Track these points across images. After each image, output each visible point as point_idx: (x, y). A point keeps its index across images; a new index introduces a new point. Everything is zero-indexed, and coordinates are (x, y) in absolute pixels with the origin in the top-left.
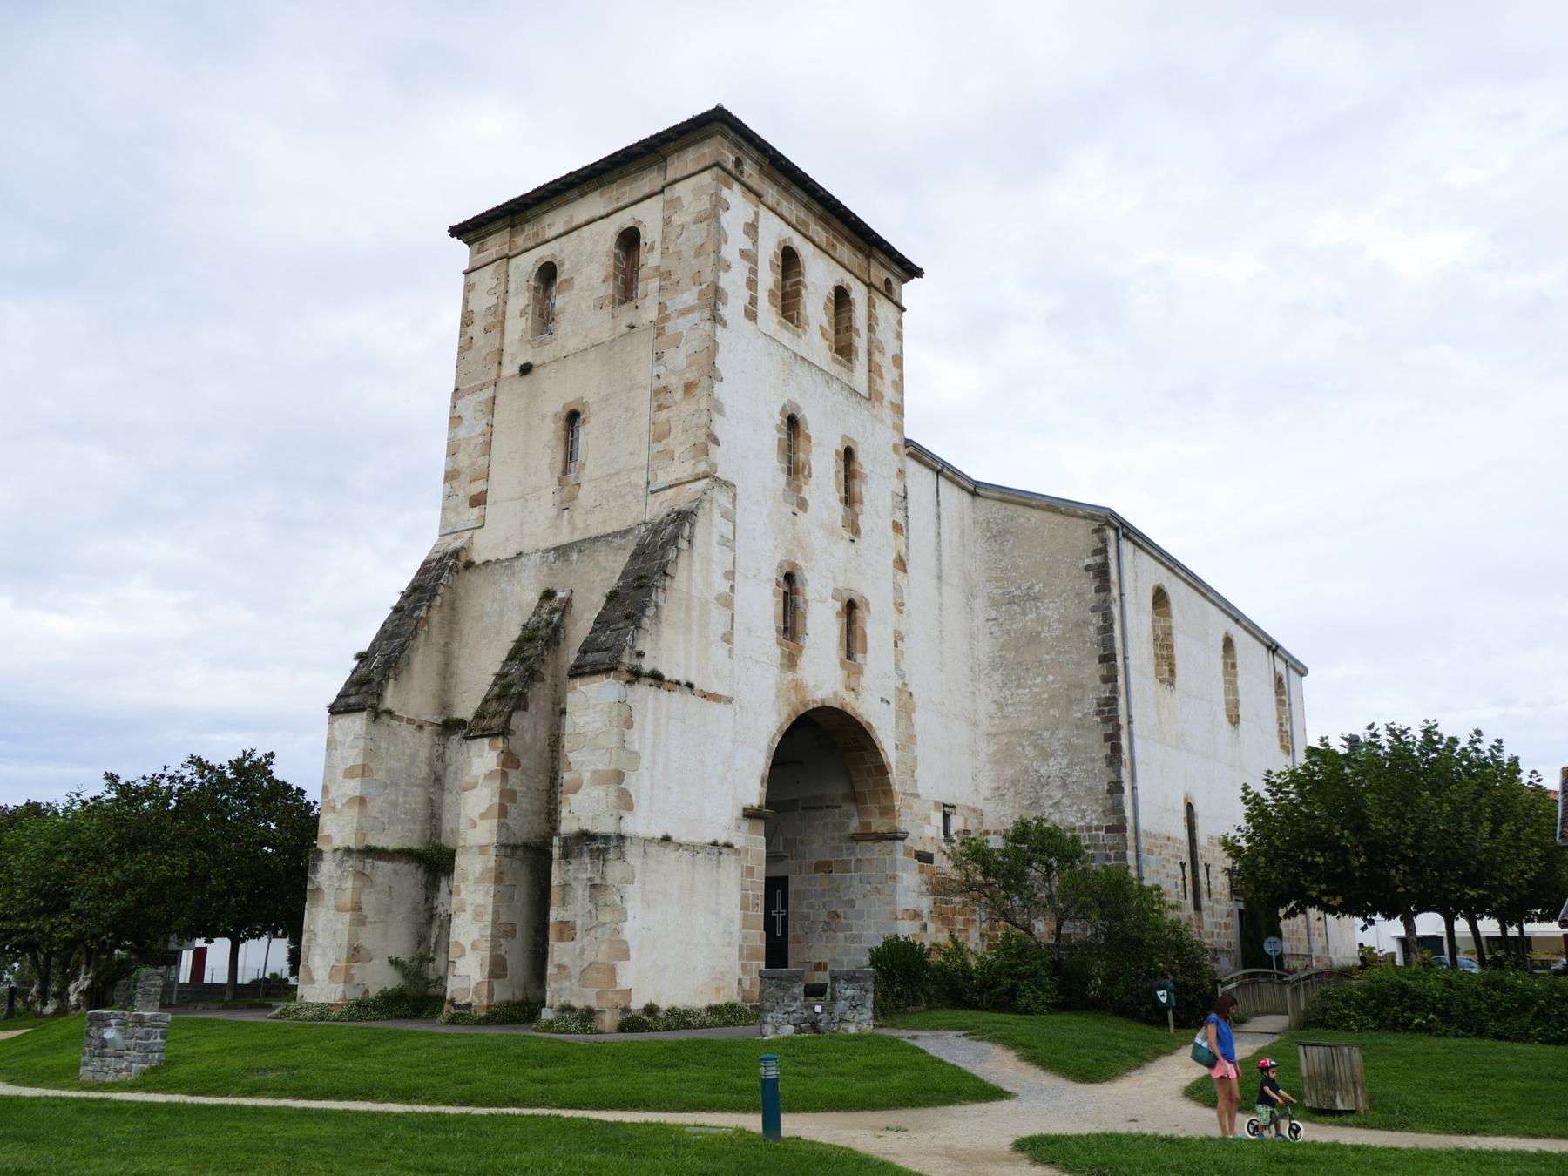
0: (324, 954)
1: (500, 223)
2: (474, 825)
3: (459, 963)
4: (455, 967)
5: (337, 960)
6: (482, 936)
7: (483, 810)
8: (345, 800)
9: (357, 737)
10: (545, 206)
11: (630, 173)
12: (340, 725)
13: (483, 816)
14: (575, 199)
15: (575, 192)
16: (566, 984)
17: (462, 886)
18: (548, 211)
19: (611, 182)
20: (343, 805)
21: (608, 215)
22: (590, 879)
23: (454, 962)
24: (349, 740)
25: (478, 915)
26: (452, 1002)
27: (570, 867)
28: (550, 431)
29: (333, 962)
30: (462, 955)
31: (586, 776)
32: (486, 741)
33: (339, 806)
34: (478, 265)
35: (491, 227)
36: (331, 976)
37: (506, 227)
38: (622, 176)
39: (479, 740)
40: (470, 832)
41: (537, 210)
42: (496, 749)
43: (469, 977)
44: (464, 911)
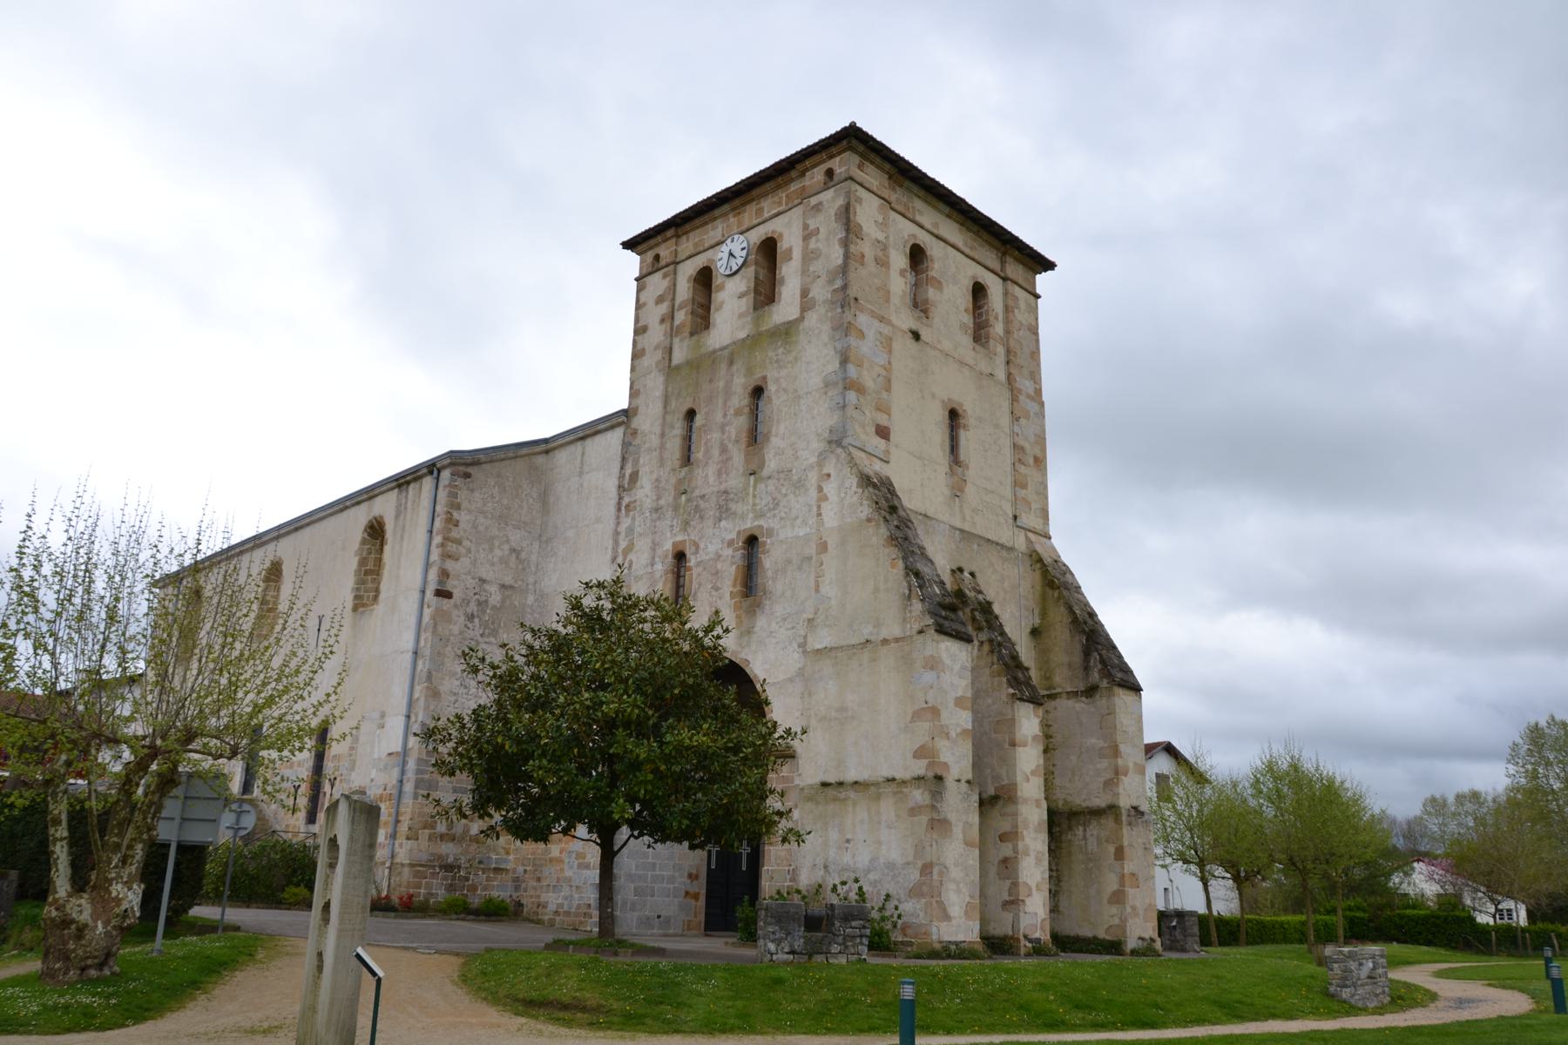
0: (958, 891)
1: (887, 166)
2: (1028, 780)
3: (1028, 901)
4: (1025, 905)
5: (971, 897)
6: (1043, 879)
7: (1033, 768)
8: (959, 730)
9: (963, 668)
10: (922, 193)
11: (980, 237)
12: (947, 647)
13: (1033, 773)
14: (939, 211)
15: (947, 210)
16: (1137, 920)
17: (1025, 833)
18: (919, 197)
19: (969, 229)
20: (957, 735)
21: (967, 256)
22: (1144, 844)
23: (1023, 901)
24: (957, 667)
25: (1038, 861)
26: (1025, 937)
27: (1134, 833)
28: (941, 416)
29: (968, 899)
30: (1029, 895)
31: (1131, 765)
32: (1031, 706)
33: (953, 734)
34: (867, 185)
35: (878, 160)
36: (966, 913)
37: (888, 173)
38: (977, 234)
39: (1027, 704)
40: (1025, 784)
41: (915, 189)
42: (1038, 717)
43: (1036, 914)
44: (1028, 855)
